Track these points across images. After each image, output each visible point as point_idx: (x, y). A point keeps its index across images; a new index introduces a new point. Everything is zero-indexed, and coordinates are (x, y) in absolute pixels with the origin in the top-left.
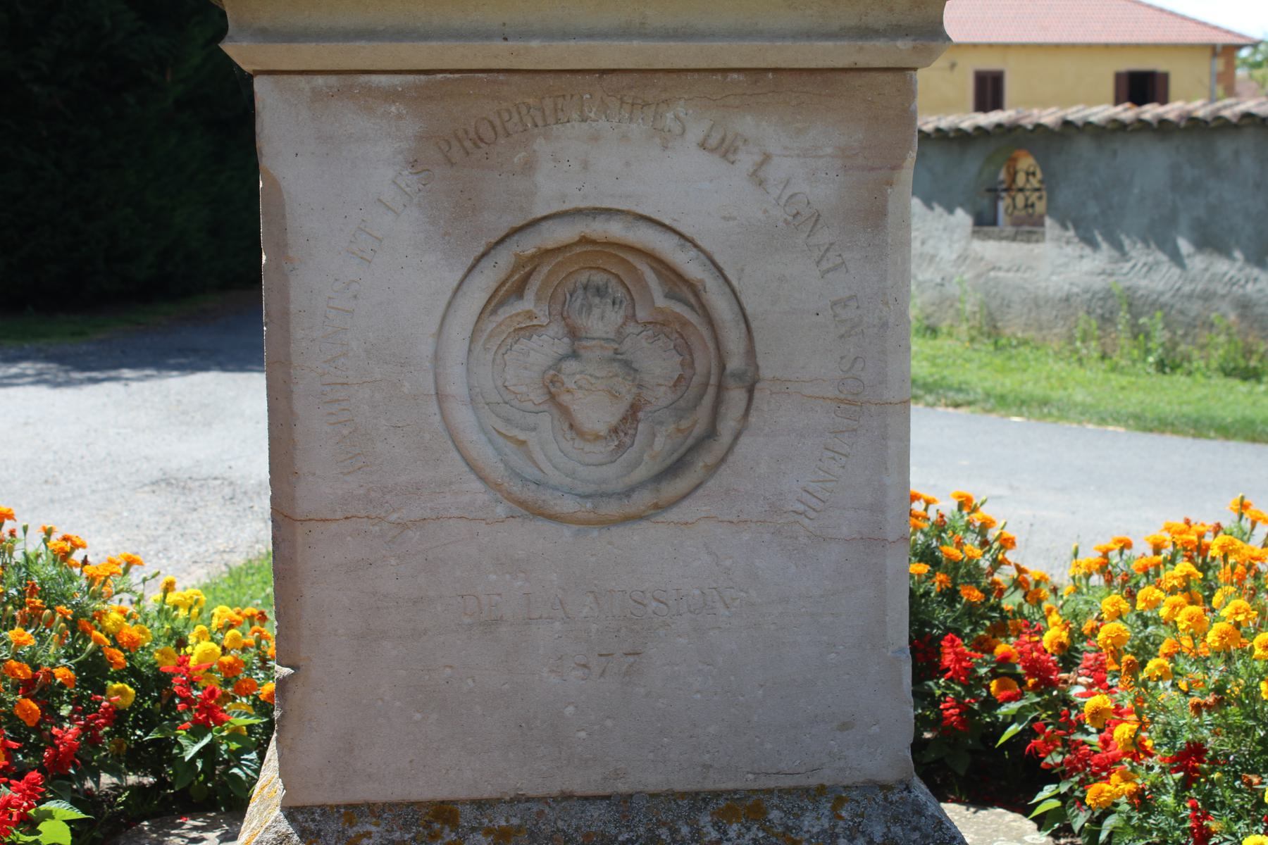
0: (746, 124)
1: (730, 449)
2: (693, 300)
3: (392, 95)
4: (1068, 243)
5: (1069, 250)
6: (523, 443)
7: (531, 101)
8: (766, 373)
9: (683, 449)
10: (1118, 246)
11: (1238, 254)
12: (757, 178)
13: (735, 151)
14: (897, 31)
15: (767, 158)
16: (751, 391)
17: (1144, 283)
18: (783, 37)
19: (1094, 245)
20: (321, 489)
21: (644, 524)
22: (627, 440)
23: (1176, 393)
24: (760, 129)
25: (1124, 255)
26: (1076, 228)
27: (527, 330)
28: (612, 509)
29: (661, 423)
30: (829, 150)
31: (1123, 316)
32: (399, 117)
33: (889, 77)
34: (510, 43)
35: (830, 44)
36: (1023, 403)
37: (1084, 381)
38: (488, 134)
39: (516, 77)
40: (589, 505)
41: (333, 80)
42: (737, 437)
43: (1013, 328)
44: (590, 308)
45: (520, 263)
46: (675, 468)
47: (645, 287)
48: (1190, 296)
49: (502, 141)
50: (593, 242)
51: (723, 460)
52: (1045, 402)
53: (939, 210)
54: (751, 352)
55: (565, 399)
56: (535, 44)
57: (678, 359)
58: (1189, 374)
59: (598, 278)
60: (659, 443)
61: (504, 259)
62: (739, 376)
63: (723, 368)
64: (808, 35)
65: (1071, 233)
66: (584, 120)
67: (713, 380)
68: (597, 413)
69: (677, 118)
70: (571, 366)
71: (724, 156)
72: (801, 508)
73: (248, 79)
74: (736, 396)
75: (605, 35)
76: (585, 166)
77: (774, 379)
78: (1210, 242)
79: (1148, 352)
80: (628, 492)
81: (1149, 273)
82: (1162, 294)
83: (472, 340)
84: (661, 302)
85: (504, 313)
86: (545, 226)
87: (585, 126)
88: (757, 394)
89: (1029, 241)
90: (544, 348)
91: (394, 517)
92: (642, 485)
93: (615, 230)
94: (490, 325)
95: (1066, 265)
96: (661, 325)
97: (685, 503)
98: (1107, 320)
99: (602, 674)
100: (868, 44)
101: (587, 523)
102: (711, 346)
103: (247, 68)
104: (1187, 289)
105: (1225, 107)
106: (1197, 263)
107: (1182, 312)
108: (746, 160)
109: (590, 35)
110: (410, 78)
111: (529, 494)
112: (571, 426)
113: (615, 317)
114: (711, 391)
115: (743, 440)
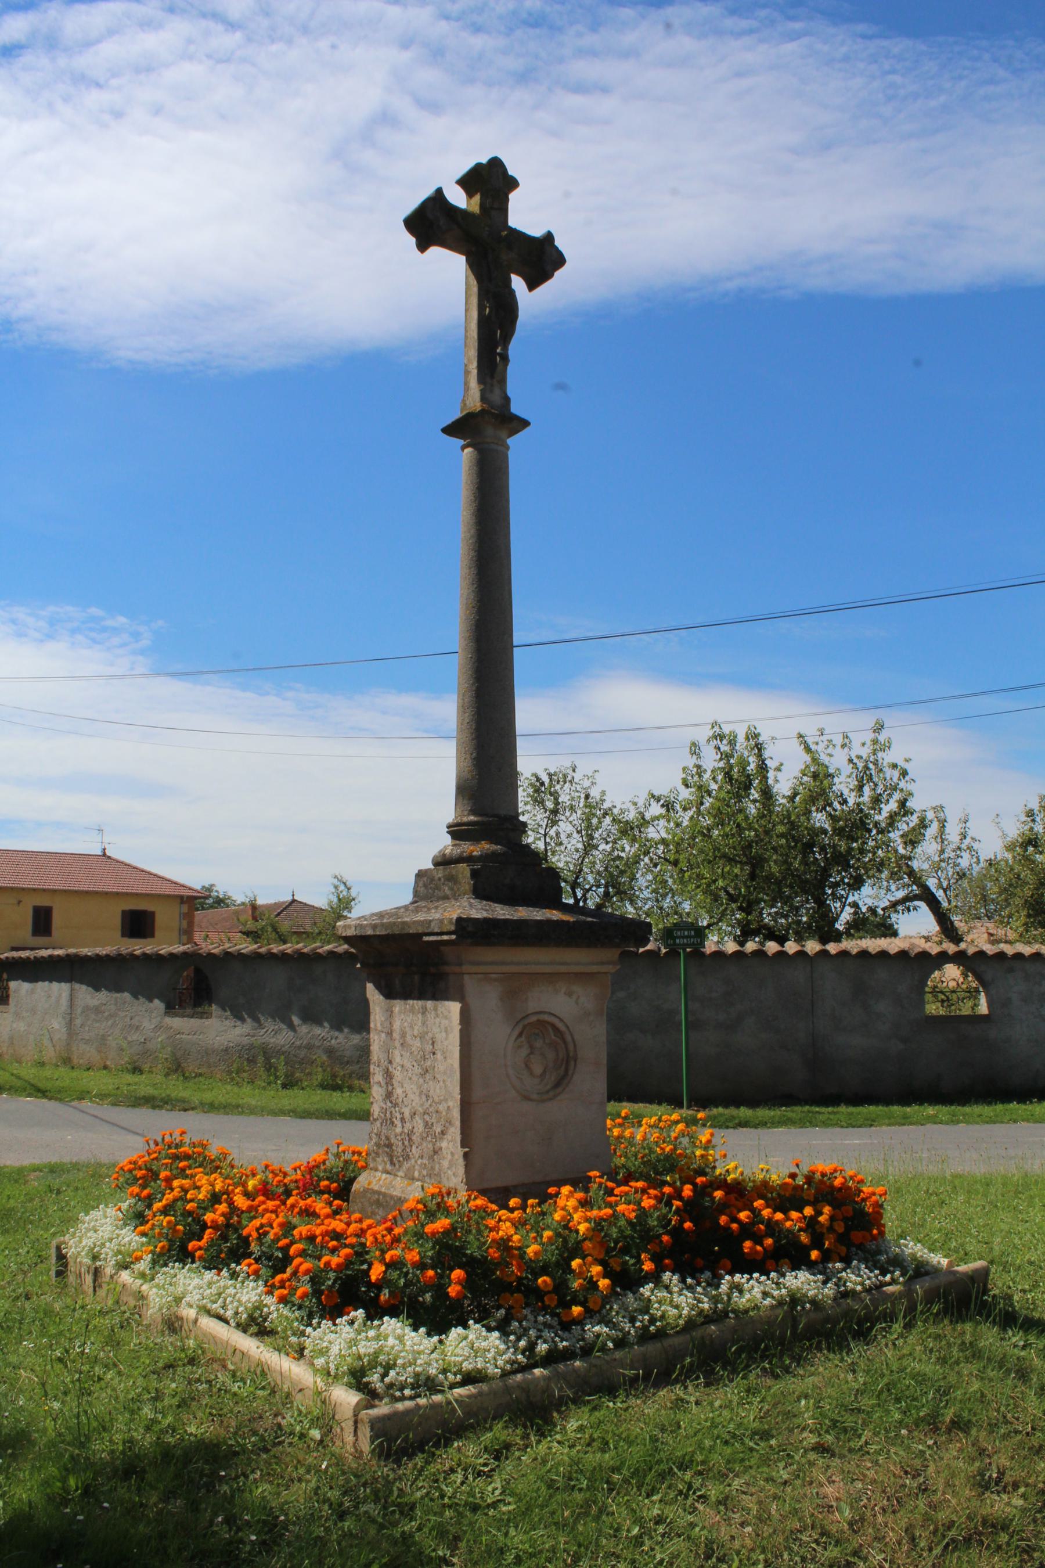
3: (495, 980)
4: (226, 1019)
5: (227, 1022)
10: (256, 1020)
11: (326, 1024)
12: (577, 1003)
16: (575, 1061)
17: (272, 1040)
19: (243, 1020)
20: (478, 1093)
23: (297, 1098)
25: (261, 1026)
26: (231, 1011)
31: (261, 1059)
36: (225, 1107)
37: (248, 1095)
43: (191, 1067)
46: (557, 1085)
48: (299, 1047)
52: (238, 1106)
53: (142, 999)
54: (575, 1051)
58: (303, 1089)
59: (537, 1031)
61: (521, 1026)
65: (229, 1013)
68: (538, 1070)
74: (572, 1063)
78: (311, 1017)
79: (277, 1078)
81: (276, 1035)
82: (283, 1046)
89: (201, 1018)
93: (546, 1017)
95: (226, 1031)
98: (252, 1061)
104: (298, 1043)
105: (317, 948)
106: (304, 1029)
107: (295, 1056)
108: (574, 997)
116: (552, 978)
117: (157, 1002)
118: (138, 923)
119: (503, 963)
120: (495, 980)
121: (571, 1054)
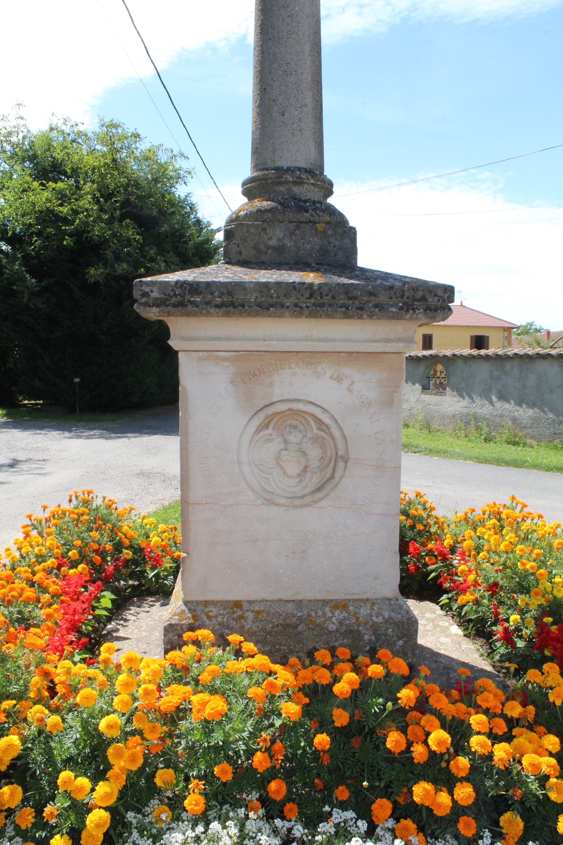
0: (346, 371)
1: (339, 482)
2: (327, 431)
3: (225, 359)
5: (454, 399)
6: (267, 479)
7: (272, 362)
8: (351, 456)
9: (322, 482)
10: (472, 398)
11: (512, 402)
12: (349, 389)
13: (342, 380)
14: (398, 340)
15: (353, 382)
16: (346, 462)
17: (480, 411)
18: (359, 341)
19: (463, 397)
20: (198, 493)
21: (309, 508)
22: (303, 478)
23: (490, 450)
24: (351, 372)
27: (269, 441)
28: (297, 502)
29: (315, 473)
30: (374, 380)
31: (473, 423)
32: (228, 366)
33: (396, 356)
34: (266, 342)
35: (375, 344)
36: (438, 452)
37: (459, 445)
38: (257, 372)
39: (268, 354)
40: (290, 501)
41: (205, 353)
42: (341, 479)
43: (435, 425)
44: (291, 433)
45: (267, 417)
46: (319, 489)
47: (310, 426)
48: (496, 416)
49: (262, 375)
50: (293, 410)
51: (336, 486)
52: (446, 452)
53: (410, 384)
55: (282, 464)
56: (275, 342)
57: (321, 451)
58: (495, 443)
59: (294, 423)
60: (314, 480)
62: (342, 457)
63: (337, 454)
64: (368, 341)
65: (456, 393)
66: (290, 368)
67: (334, 458)
68: (293, 469)
69: (322, 368)
70: (284, 453)
71: (338, 381)
72: (362, 503)
73: (176, 353)
74: (341, 464)
75: (299, 340)
76: (291, 384)
77: (354, 459)
78: (503, 397)
79: (481, 435)
80: (303, 497)
81: (482, 408)
82: (486, 415)
83: (250, 443)
84: (315, 431)
85: (262, 434)
86: (276, 404)
87: (291, 370)
88: (348, 464)
90: (276, 445)
91: (223, 503)
92: (308, 494)
94: (257, 438)
95: (453, 404)
96: (316, 439)
97: (323, 501)
98: (467, 423)
99: (293, 559)
100: (389, 344)
101: (289, 507)
102: (333, 446)
103: (176, 349)
104: (495, 413)
106: (498, 404)
107: (493, 421)
108: (346, 383)
109: (293, 340)
110: (232, 353)
111: (269, 497)
112: (284, 473)
113: (299, 436)
114: (333, 462)
115: (343, 479)
116: (310, 357)
117: (417, 385)
118: (479, 342)
119: (228, 339)
120: (225, 359)
121: (340, 453)
